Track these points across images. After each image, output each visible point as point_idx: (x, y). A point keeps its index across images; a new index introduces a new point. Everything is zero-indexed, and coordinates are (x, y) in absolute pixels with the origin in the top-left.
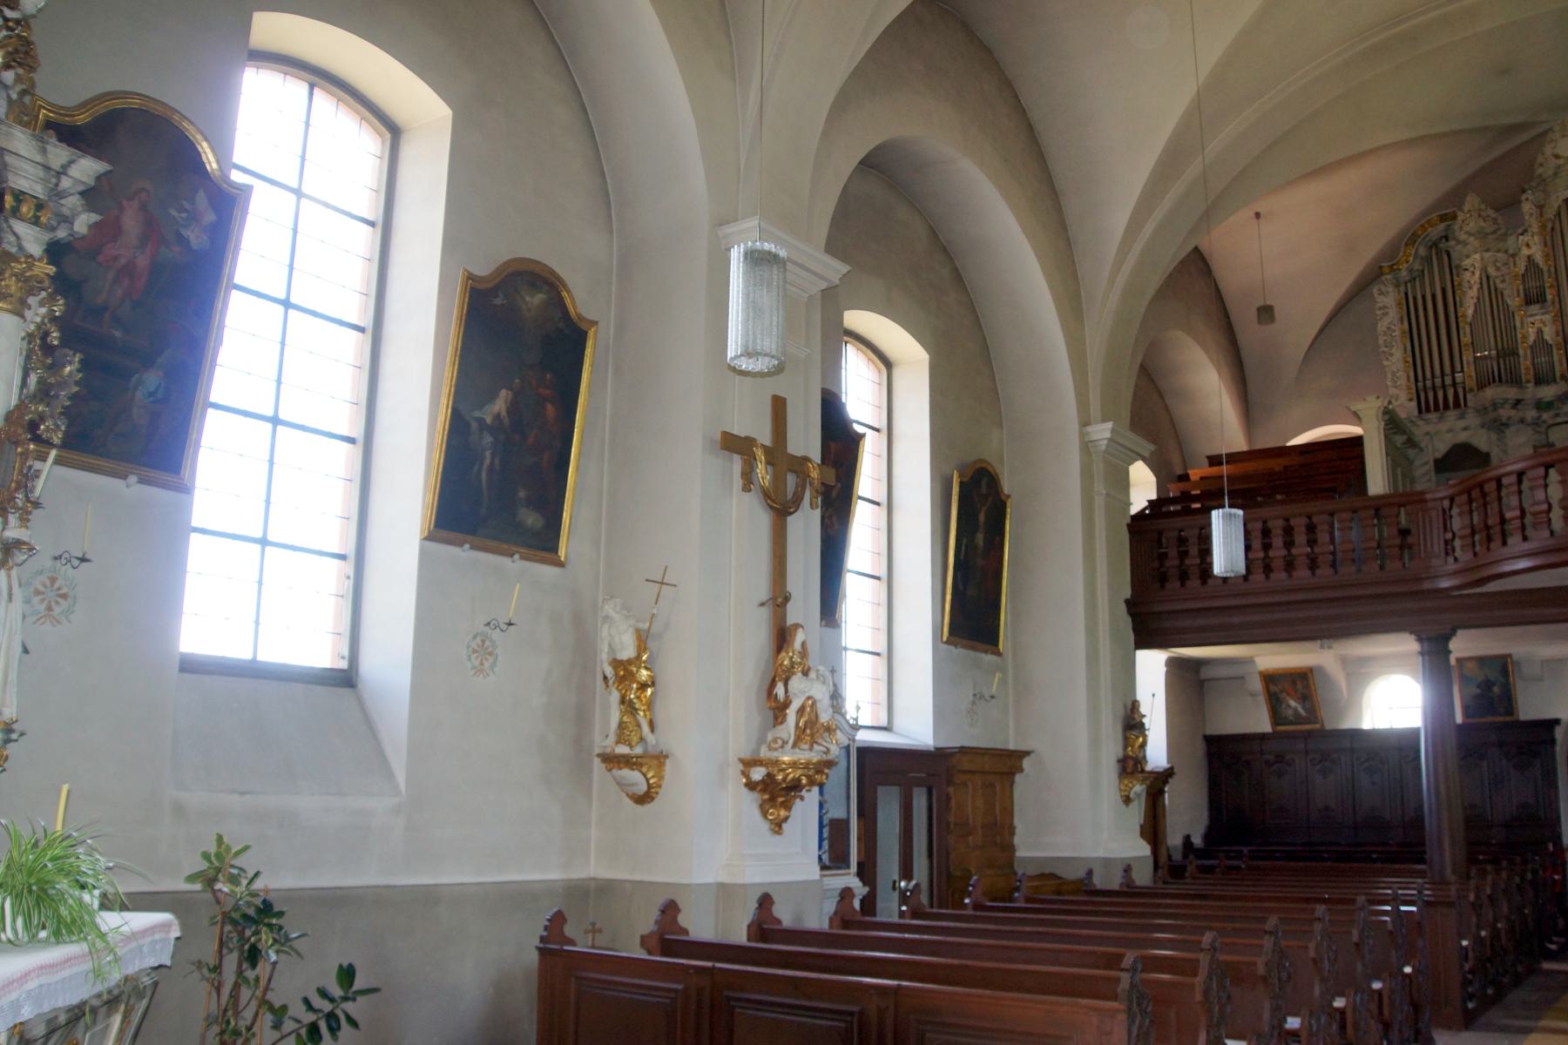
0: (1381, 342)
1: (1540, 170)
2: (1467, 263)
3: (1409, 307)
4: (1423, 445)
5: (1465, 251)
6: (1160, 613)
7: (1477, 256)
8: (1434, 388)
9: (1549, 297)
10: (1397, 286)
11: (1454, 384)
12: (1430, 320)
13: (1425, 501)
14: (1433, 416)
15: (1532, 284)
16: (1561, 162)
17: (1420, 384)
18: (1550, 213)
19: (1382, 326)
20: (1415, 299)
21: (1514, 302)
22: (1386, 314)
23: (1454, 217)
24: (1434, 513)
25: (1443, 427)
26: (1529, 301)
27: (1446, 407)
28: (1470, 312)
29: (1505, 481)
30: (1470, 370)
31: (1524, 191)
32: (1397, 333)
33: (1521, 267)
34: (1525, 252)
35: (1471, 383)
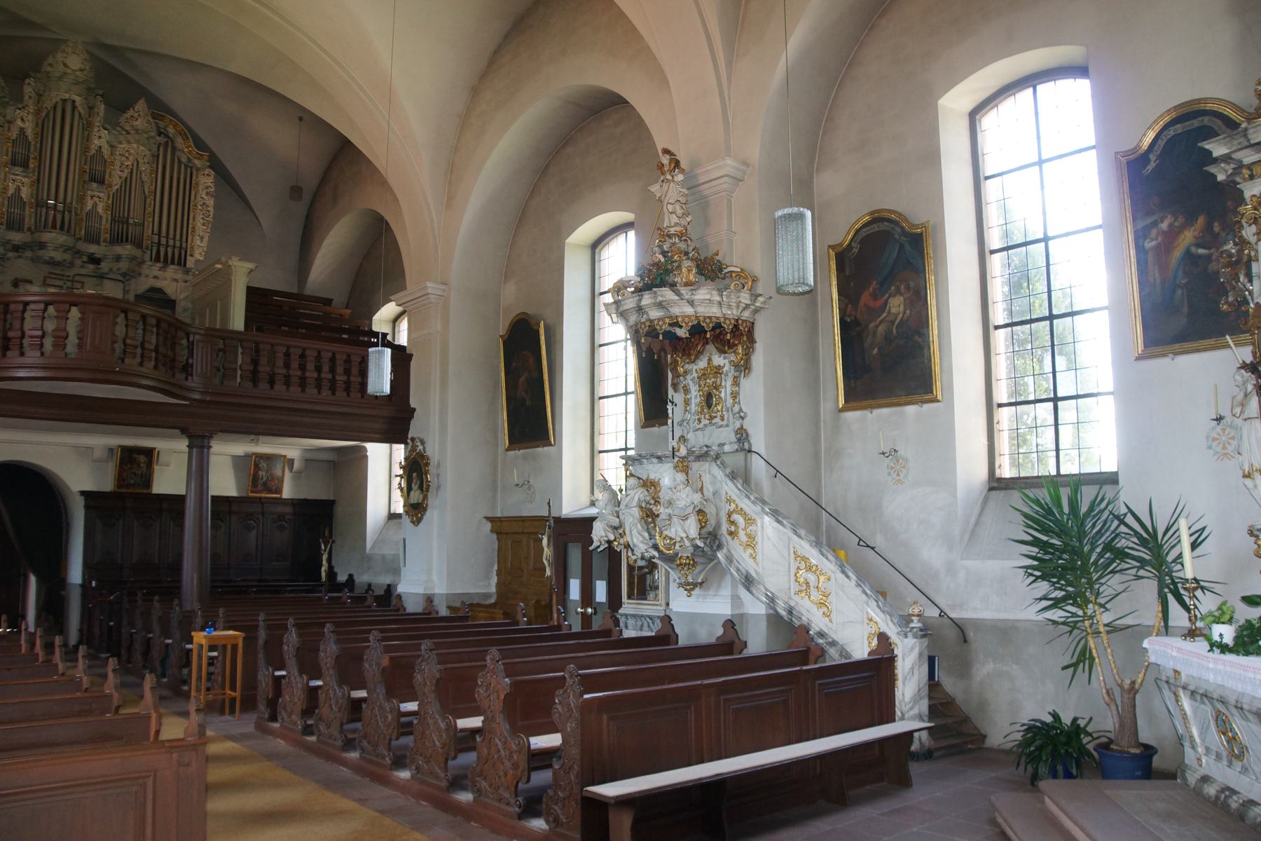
1: (49, 69)
18: (48, 104)
33: (14, 134)
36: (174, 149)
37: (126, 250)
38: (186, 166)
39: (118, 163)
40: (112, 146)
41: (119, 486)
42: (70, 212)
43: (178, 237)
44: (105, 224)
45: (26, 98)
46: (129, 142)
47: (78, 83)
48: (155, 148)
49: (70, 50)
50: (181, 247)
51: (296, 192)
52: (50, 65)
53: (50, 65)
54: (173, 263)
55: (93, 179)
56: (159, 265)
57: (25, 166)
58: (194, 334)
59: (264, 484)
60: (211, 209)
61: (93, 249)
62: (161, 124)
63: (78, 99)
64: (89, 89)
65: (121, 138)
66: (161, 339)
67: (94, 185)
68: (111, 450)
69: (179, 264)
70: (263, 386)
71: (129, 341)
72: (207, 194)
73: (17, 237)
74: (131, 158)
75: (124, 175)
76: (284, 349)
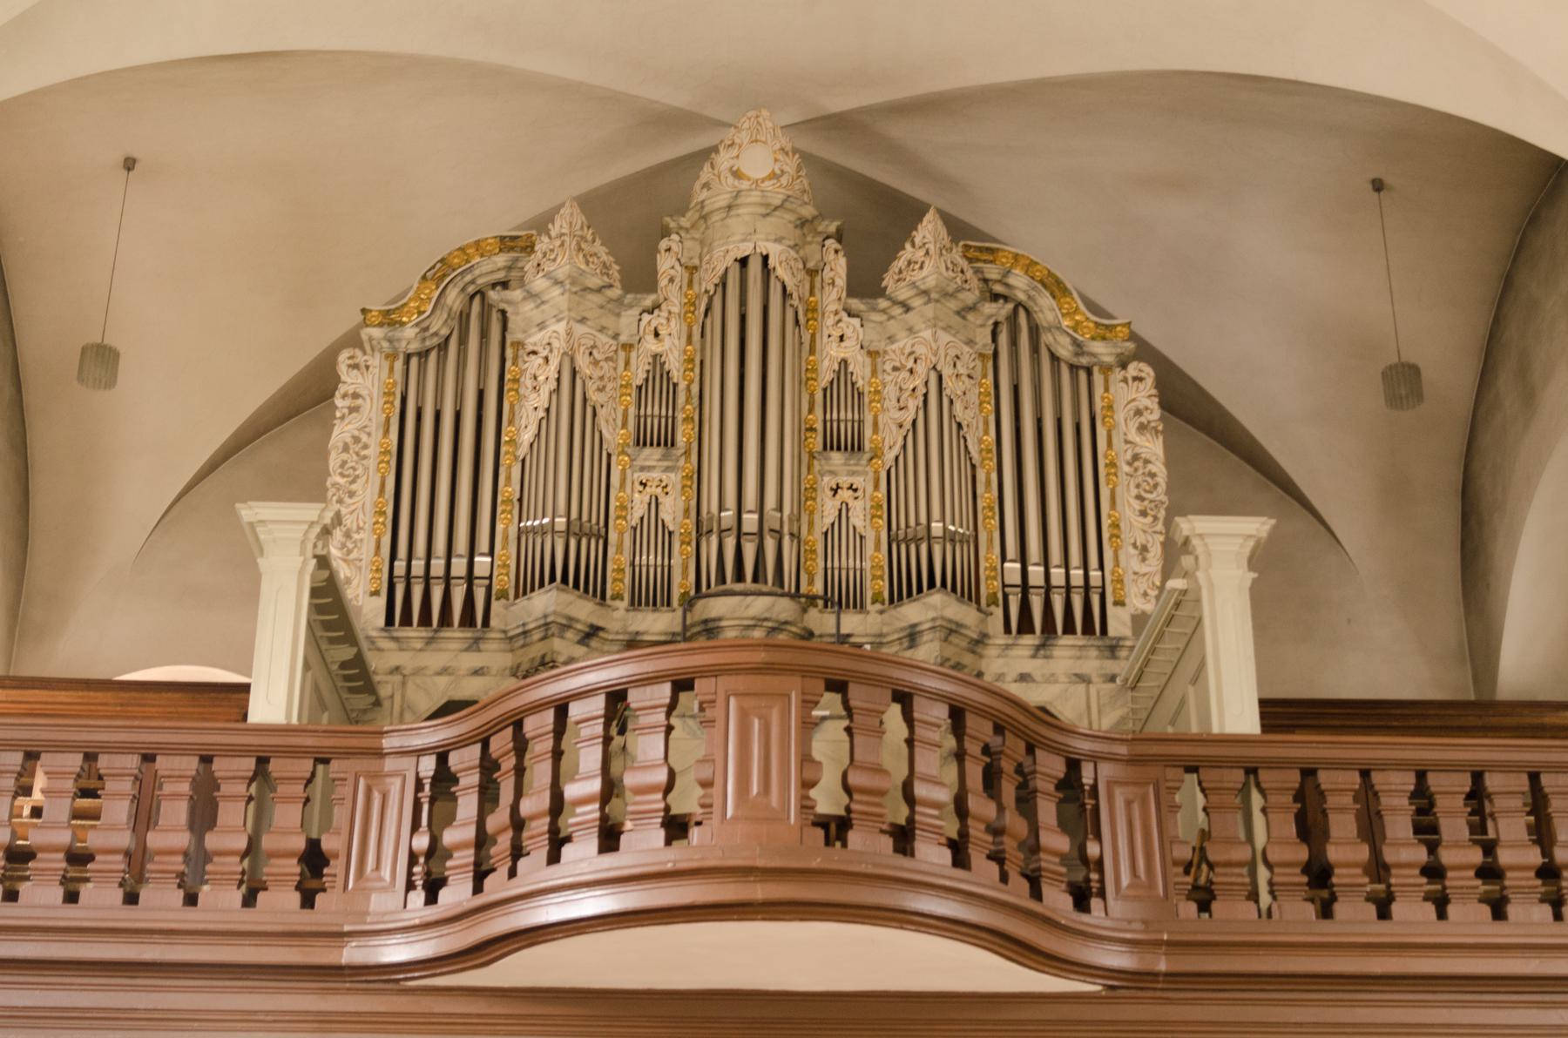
0: (334, 461)
1: (704, 194)
2: (535, 339)
3: (405, 417)
4: (384, 692)
5: (537, 316)
7: (561, 327)
8: (427, 577)
9: (681, 440)
10: (392, 357)
11: (470, 577)
12: (445, 445)
13: (380, 754)
14: (415, 633)
15: (654, 409)
16: (745, 185)
17: (400, 567)
18: (708, 281)
19: (342, 432)
21: (615, 435)
23: (529, 248)
24: (394, 785)
25: (434, 660)
26: (641, 441)
28: (527, 437)
29: (576, 710)
30: (507, 553)
31: (666, 233)
34: (651, 345)
35: (505, 580)
36: (1035, 331)
37: (932, 607)
38: (1074, 368)
39: (890, 392)
40: (873, 354)
42: (778, 534)
43: (1075, 558)
44: (874, 556)
45: (663, 282)
46: (911, 330)
48: (984, 337)
49: (744, 137)
50: (1087, 587)
51: (1403, 382)
52: (706, 186)
53: (706, 186)
54: (1069, 628)
56: (1029, 640)
57: (668, 442)
58: (1095, 758)
60: (1159, 468)
62: (992, 272)
63: (775, 251)
64: (803, 223)
65: (893, 327)
67: (837, 457)
69: (1088, 629)
70: (1354, 914)
71: (855, 779)
72: (1142, 428)
74: (921, 369)
75: (908, 417)
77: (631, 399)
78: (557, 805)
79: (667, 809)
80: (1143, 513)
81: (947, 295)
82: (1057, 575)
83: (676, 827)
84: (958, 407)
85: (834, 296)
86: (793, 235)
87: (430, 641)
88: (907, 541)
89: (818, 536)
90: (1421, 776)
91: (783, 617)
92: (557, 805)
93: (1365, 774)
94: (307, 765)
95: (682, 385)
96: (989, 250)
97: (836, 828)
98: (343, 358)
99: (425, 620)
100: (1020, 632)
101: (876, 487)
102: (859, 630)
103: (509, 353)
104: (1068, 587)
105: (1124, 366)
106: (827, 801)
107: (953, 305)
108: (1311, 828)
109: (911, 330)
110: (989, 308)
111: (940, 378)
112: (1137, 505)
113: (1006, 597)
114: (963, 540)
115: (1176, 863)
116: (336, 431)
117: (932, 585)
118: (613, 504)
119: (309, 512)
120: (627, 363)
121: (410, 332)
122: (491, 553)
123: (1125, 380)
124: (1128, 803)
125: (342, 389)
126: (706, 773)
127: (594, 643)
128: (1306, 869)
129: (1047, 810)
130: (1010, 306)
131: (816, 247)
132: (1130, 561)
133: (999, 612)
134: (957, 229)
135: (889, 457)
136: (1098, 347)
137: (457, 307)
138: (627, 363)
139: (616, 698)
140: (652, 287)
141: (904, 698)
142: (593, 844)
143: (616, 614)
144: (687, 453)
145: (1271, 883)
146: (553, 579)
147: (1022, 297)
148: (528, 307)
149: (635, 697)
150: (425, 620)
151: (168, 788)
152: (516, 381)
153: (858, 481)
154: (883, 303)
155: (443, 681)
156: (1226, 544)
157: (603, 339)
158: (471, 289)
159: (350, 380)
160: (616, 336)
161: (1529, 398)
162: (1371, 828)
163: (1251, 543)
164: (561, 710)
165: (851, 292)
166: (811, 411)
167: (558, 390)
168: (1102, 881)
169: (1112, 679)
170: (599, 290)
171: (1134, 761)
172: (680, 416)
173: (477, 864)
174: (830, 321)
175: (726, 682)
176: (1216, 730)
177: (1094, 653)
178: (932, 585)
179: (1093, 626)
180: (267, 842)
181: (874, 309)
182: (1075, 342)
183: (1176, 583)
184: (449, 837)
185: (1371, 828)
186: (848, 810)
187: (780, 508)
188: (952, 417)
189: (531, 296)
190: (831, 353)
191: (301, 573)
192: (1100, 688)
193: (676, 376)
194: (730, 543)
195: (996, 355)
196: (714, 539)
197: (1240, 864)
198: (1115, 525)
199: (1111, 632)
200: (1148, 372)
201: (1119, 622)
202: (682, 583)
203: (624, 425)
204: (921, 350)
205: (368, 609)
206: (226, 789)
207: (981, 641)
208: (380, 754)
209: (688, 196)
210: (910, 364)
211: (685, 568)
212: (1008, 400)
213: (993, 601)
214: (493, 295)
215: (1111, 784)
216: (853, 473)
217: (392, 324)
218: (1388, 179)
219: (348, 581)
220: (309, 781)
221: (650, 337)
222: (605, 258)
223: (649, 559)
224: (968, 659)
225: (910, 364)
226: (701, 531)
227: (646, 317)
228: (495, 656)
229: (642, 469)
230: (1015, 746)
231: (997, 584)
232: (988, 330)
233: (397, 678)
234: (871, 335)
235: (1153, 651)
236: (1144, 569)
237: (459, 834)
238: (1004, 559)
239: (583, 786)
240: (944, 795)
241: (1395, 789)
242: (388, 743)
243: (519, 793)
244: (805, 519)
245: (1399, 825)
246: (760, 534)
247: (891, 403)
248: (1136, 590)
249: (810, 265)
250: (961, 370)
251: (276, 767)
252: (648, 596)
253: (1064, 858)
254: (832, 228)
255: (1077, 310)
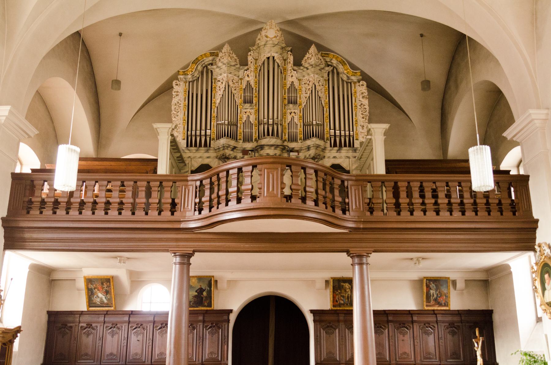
0: (173, 108)
1: (259, 41)
2: (219, 78)
3: (189, 96)
4: (187, 162)
6: (22, 228)
7: (225, 75)
8: (196, 135)
9: (254, 102)
10: (186, 82)
11: (206, 135)
13: (187, 181)
14: (193, 148)
16: (268, 39)
17: (189, 133)
18: (260, 63)
19: (174, 101)
20: (193, 94)
21: (239, 101)
22: (177, 95)
23: (217, 55)
24: (191, 188)
25: (198, 155)
26: (245, 102)
27: (200, 145)
28: (218, 101)
29: (231, 172)
30: (214, 129)
31: (250, 51)
32: (182, 105)
34: (247, 79)
35: (214, 136)
36: (338, 74)
38: (347, 83)
39: (304, 89)
40: (299, 80)
41: (334, 306)
42: (277, 124)
45: (249, 63)
46: (308, 74)
47: (275, 45)
48: (326, 75)
49: (268, 27)
50: (350, 135)
51: (426, 85)
52: (259, 39)
53: (259, 39)
54: (345, 146)
55: (290, 102)
56: (336, 148)
57: (251, 102)
58: (348, 180)
59: (435, 300)
60: (367, 107)
61: (293, 145)
62: (328, 59)
63: (276, 56)
65: (304, 73)
66: (321, 185)
67: (291, 105)
68: (327, 282)
69: (350, 146)
70: (405, 214)
71: (293, 187)
72: (363, 97)
73: (249, 146)
74: (311, 84)
75: (308, 95)
76: (418, 184)
77: (242, 92)
78: (227, 193)
79: (251, 194)
80: (363, 118)
81: (317, 66)
82: (343, 133)
83: (253, 198)
84: (319, 92)
85: (290, 66)
86: (280, 51)
87: (197, 150)
88: (307, 125)
89: (287, 124)
90: (421, 183)
91: (279, 144)
92: (227, 193)
93: (409, 183)
94: (171, 183)
95: (254, 88)
96: (328, 54)
97: (289, 198)
98: (174, 83)
99: (196, 146)
100: (334, 146)
101: (300, 112)
102: (296, 147)
103: (213, 81)
104: (345, 136)
105: (359, 82)
106: (287, 192)
107: (318, 68)
108: (396, 195)
109: (308, 74)
110: (327, 68)
111: (315, 86)
112: (362, 116)
113: (330, 138)
114: (321, 125)
115: (365, 203)
116: (173, 100)
117: (313, 136)
118: (239, 117)
119: (169, 125)
120: (241, 83)
121: (190, 76)
122: (210, 129)
123: (359, 86)
124: (355, 190)
125: (174, 90)
126: (260, 186)
127: (235, 150)
128: (395, 204)
129: (337, 192)
130: (332, 68)
131: (286, 54)
132: (360, 129)
133: (329, 142)
134: (321, 48)
135: (303, 105)
136: (353, 78)
137: (200, 70)
138: (241, 83)
139: (240, 170)
140: (247, 65)
141: (304, 168)
142: (235, 202)
143: (241, 143)
144: (256, 105)
145: (387, 208)
146: (225, 136)
147: (335, 65)
148: (218, 69)
149: (244, 169)
150: (196, 146)
151: (140, 189)
152: (215, 88)
153: (296, 111)
154: (302, 68)
155: (200, 159)
156: (379, 130)
157: (235, 78)
158: (204, 65)
159: (176, 88)
160: (238, 77)
161: (457, 87)
162: (409, 195)
163: (385, 130)
164: (228, 172)
165: (294, 65)
166: (285, 94)
167: (225, 90)
168: (349, 208)
169: (355, 157)
170: (234, 66)
171: (356, 180)
172: (254, 96)
173: (210, 205)
174: (289, 72)
175: (264, 166)
176: (375, 173)
177: (351, 151)
178: (313, 136)
179: (351, 145)
180: (163, 201)
181: (300, 69)
182: (348, 77)
183: (369, 137)
184: (203, 199)
185: (409, 195)
186: (291, 194)
187: (278, 118)
188: (318, 95)
189: (218, 67)
190: (289, 80)
191: (168, 139)
192: (352, 159)
193: (253, 86)
194: (266, 126)
195: (329, 79)
196: (262, 126)
197: (380, 203)
198: (356, 121)
199: (355, 146)
200: (365, 83)
201: (357, 144)
202: (255, 136)
203: (241, 98)
204: (311, 79)
205: (182, 143)
206: (153, 189)
207: (324, 149)
208: (187, 181)
209: (255, 42)
210: (308, 83)
211: (256, 132)
212: (331, 90)
213: (327, 139)
214: (209, 67)
215: (351, 186)
216: (295, 109)
217: (185, 74)
218: (424, 34)
219: (177, 136)
220: (172, 187)
221: (246, 77)
222: (235, 58)
223: (247, 130)
224: (321, 153)
225: (308, 83)
226: (259, 124)
227: (245, 72)
228: (212, 154)
229: (245, 109)
230: (330, 178)
231: (328, 135)
232: (327, 74)
233: (190, 159)
234: (299, 75)
235: (363, 152)
236: (363, 131)
237: (206, 199)
238: (330, 129)
239: (233, 189)
240: (313, 190)
241: (415, 187)
242: (189, 178)
243: (219, 190)
244: (283, 120)
245: (416, 194)
246: (273, 124)
247: (304, 92)
248: (361, 138)
249: (285, 58)
250: (320, 84)
251: (164, 184)
252: (248, 139)
253: (340, 203)
254: (290, 49)
255: (348, 69)
